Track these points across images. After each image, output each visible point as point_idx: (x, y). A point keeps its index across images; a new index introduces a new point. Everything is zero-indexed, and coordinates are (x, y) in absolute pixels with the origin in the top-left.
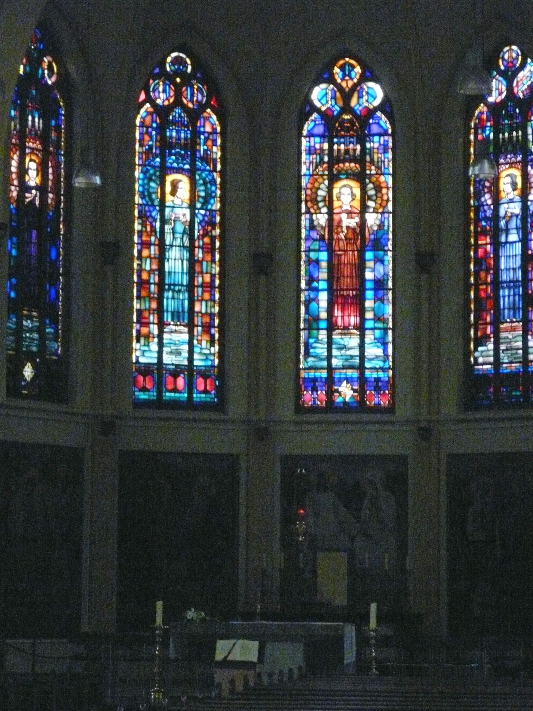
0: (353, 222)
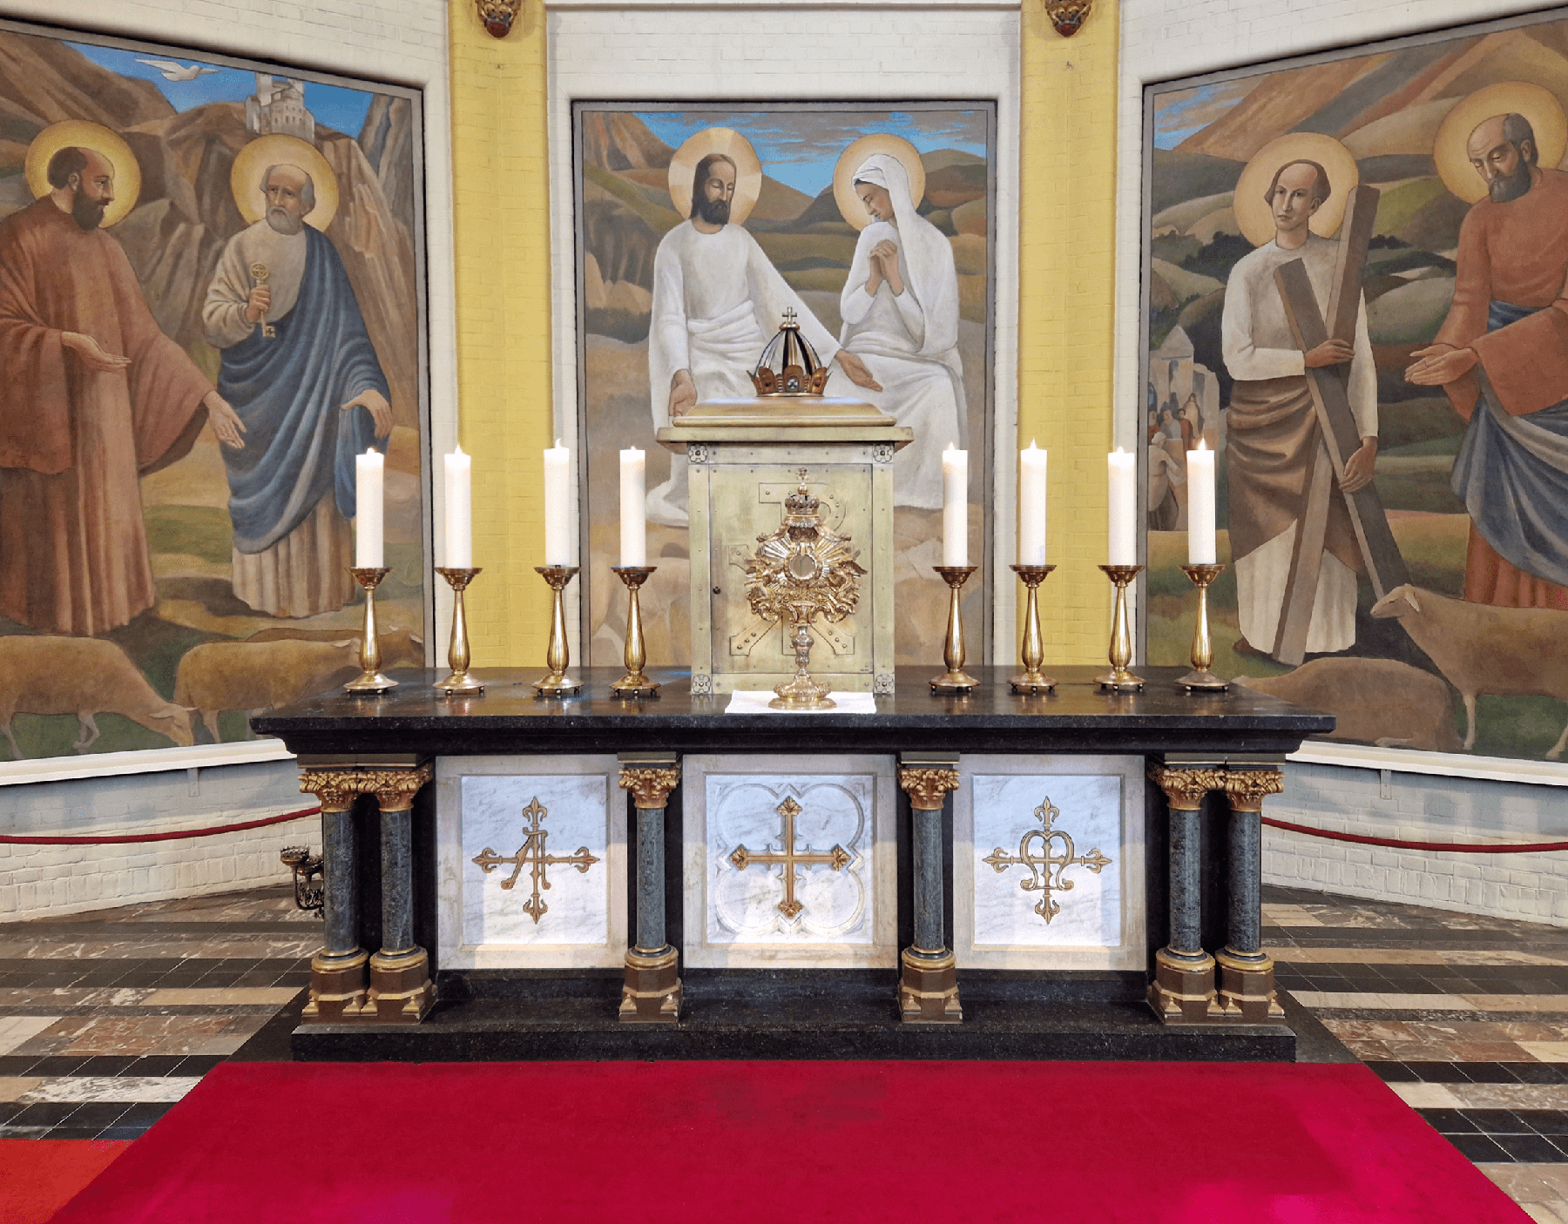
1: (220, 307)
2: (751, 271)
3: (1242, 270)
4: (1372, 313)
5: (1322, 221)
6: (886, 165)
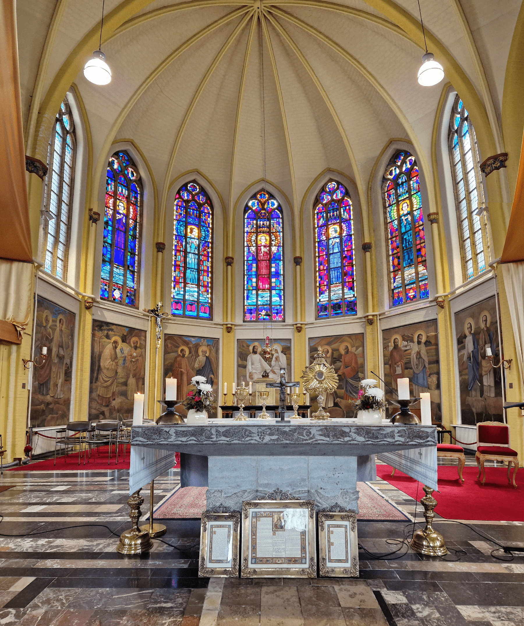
0: (266, 250)
1: (196, 366)
2: (260, 359)
5: (328, 355)
6: (278, 347)
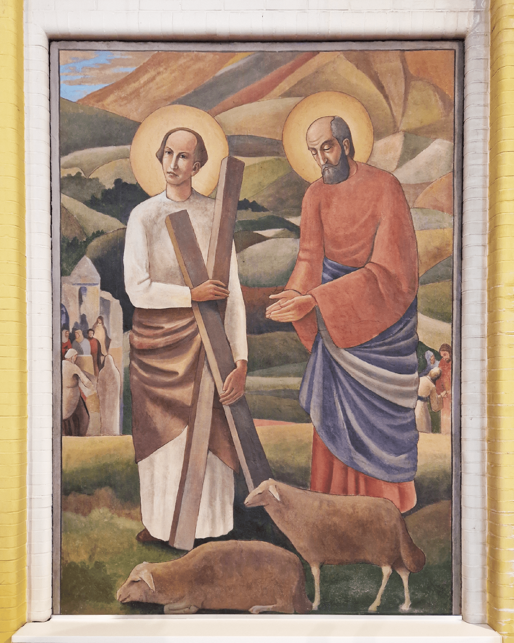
3: (139, 213)
4: (242, 262)
5: (203, 180)
